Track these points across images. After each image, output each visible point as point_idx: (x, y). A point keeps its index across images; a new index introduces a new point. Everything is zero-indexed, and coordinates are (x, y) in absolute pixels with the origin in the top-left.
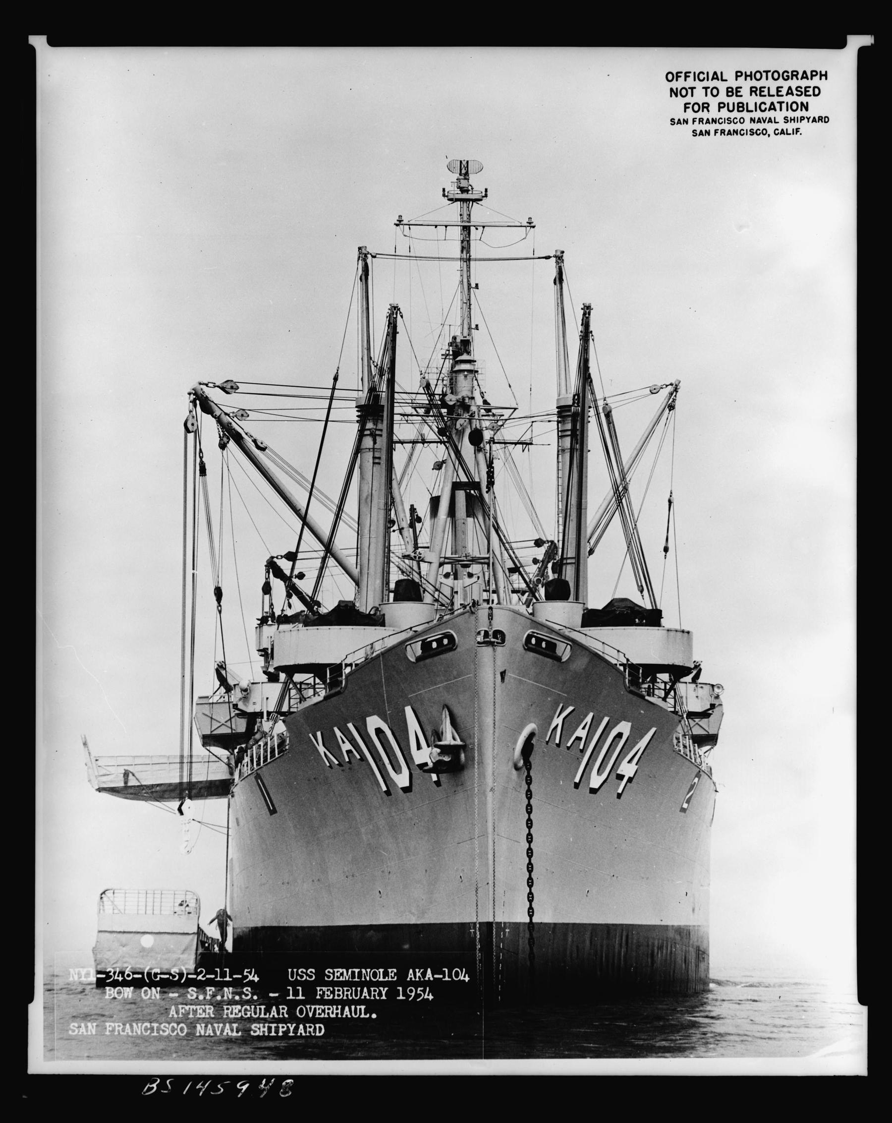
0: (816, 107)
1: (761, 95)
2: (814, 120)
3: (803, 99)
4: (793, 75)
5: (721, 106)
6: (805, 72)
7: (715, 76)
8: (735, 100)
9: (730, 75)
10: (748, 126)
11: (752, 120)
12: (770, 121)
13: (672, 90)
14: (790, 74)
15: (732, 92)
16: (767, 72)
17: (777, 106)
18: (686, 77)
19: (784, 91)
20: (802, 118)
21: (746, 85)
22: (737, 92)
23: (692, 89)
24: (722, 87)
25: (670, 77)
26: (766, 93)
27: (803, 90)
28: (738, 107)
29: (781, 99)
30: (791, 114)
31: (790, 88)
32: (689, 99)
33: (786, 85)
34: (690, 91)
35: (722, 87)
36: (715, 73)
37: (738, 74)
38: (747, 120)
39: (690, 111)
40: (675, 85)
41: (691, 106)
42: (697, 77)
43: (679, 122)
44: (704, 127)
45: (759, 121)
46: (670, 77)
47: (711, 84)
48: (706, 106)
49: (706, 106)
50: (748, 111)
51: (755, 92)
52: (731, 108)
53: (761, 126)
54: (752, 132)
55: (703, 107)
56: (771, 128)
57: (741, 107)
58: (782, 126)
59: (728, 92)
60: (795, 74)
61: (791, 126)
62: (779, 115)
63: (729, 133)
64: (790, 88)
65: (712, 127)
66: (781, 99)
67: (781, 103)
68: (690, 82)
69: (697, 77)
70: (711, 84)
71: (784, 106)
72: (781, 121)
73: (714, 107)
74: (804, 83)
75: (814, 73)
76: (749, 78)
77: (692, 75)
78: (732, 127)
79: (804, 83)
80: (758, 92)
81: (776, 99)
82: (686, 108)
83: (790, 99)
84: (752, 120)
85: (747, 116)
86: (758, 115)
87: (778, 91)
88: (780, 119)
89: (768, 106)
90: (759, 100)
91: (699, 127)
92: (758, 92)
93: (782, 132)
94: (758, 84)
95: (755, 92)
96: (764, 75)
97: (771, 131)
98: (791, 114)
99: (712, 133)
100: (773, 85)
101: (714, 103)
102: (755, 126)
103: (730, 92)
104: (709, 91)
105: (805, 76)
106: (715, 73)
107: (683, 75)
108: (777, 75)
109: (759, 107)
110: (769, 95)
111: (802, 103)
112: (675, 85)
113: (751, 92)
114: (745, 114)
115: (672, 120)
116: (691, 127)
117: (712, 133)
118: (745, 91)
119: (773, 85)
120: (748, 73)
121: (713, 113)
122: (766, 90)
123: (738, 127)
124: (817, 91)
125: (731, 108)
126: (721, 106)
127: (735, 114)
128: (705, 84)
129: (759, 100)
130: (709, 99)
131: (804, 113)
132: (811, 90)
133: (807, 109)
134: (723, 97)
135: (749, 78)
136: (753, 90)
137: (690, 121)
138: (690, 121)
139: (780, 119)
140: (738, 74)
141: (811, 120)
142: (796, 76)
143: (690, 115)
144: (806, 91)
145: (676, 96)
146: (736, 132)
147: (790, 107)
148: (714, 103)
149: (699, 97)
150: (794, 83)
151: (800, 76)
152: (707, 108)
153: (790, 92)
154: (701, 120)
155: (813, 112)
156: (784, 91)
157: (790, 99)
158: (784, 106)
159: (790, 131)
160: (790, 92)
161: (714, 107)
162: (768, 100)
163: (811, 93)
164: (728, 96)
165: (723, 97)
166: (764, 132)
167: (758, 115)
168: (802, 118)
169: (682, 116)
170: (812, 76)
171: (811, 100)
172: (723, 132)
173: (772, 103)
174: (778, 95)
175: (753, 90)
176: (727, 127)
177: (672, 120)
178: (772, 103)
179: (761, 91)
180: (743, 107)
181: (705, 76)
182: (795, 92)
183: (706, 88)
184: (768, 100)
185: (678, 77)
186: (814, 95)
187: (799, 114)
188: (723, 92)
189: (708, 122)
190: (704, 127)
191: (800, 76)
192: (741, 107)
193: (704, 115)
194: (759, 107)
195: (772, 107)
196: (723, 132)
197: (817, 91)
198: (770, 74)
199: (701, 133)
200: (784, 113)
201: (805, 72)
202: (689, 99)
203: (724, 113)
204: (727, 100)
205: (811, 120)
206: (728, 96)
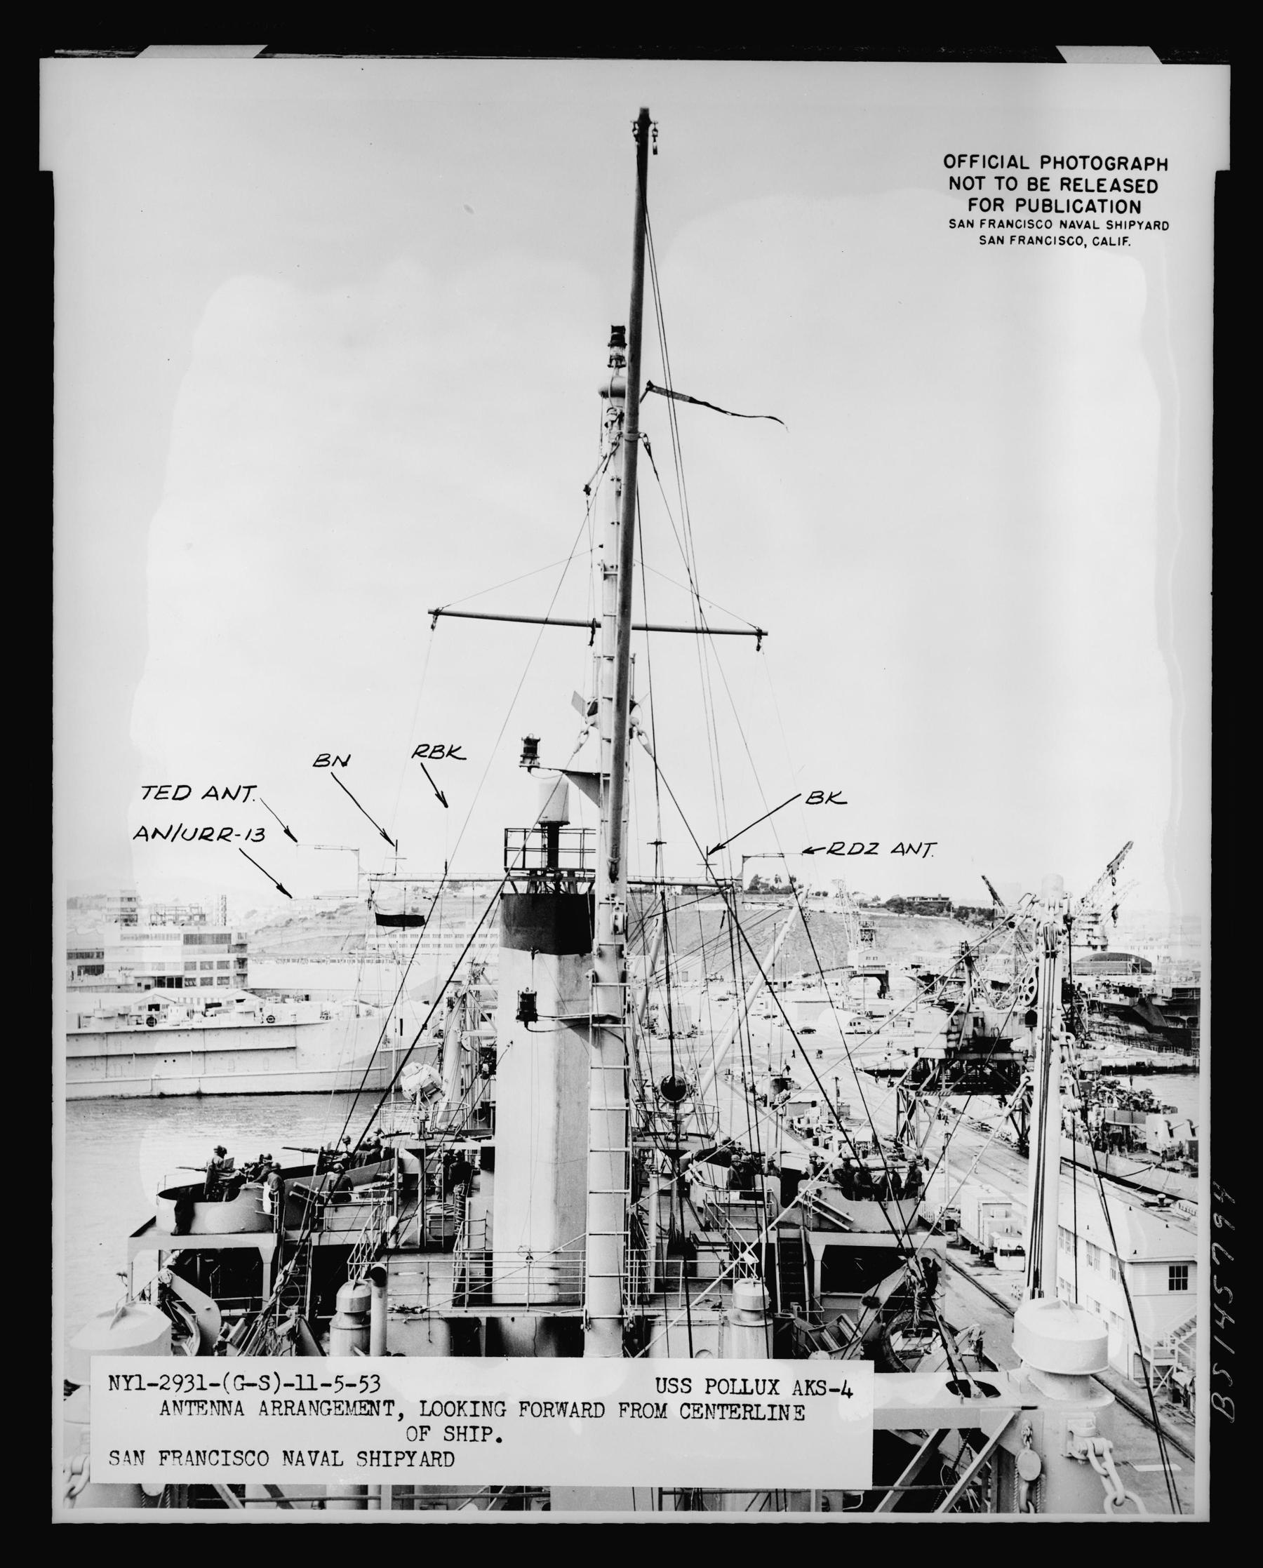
0: (1152, 207)
1: (1075, 190)
2: (1148, 226)
3: (1133, 196)
4: (1120, 163)
5: (1020, 203)
6: (1137, 159)
7: (1013, 162)
8: (1039, 195)
9: (1033, 162)
10: (1056, 231)
11: (1063, 224)
12: (1087, 225)
13: (952, 179)
14: (1116, 162)
15: (1035, 184)
16: (1084, 158)
17: (1098, 205)
18: (972, 161)
19: (1107, 185)
20: (1132, 224)
21: (1055, 175)
22: (1042, 184)
23: (980, 178)
24: (1022, 176)
25: (950, 161)
26: (1082, 187)
27: (1134, 184)
28: (1044, 205)
29: (1102, 196)
30: (1116, 218)
31: (1116, 181)
32: (975, 192)
33: (1110, 176)
34: (977, 181)
35: (1022, 176)
36: (1013, 158)
37: (1045, 160)
38: (1056, 224)
39: (976, 209)
40: (958, 172)
41: (978, 202)
42: (988, 162)
43: (961, 224)
44: (996, 232)
45: (1072, 225)
46: (950, 161)
47: (1007, 172)
48: (999, 204)
49: (999, 204)
50: (1057, 211)
51: (1068, 185)
52: (1033, 207)
53: (1075, 232)
54: (1063, 241)
55: (995, 205)
56: (1088, 235)
57: (1047, 205)
58: (1103, 232)
59: (1030, 184)
60: (1123, 162)
61: (1116, 234)
62: (1100, 218)
63: (1031, 241)
64: (1116, 181)
65: (1007, 232)
66: (1102, 196)
67: (1103, 201)
68: (978, 169)
69: (988, 162)
70: (1007, 172)
71: (1107, 205)
72: (1103, 226)
73: (1010, 205)
74: (1135, 175)
75: (1149, 162)
76: (1059, 166)
77: (980, 159)
78: (1035, 233)
79: (1135, 175)
80: (1071, 186)
81: (1096, 196)
82: (971, 205)
83: (1115, 196)
84: (1063, 224)
85: (1055, 218)
86: (1070, 217)
87: (1099, 185)
88: (1101, 223)
89: (1085, 205)
90: (1073, 196)
91: (989, 232)
92: (1071, 186)
93: (1104, 242)
94: (1072, 175)
95: (1068, 185)
96: (1081, 161)
97: (1088, 240)
98: (1116, 218)
99: (1007, 240)
100: (1092, 176)
101: (1010, 198)
102: (1067, 232)
103: (1033, 184)
104: (1004, 182)
105: (1136, 165)
106: (1013, 158)
107: (968, 159)
108: (1098, 162)
109: (1072, 206)
110: (1087, 190)
111: (1132, 203)
112: (958, 172)
113: (1062, 184)
114: (1053, 215)
115: (952, 221)
116: (977, 231)
117: (1007, 240)
118: (1053, 184)
119: (1092, 176)
120: (1059, 159)
121: (1009, 213)
122: (1083, 183)
123: (1043, 233)
124: (1153, 186)
125: (1033, 207)
126: (1020, 203)
127: (1039, 214)
128: (999, 172)
129: (1073, 196)
130: (1004, 193)
131: (1134, 216)
132: (1145, 184)
133: (1138, 211)
134: (1022, 191)
135: (1059, 166)
136: (1065, 183)
137: (977, 224)
138: (977, 224)
139: (1101, 223)
140: (1045, 160)
141: (1144, 226)
142: (1125, 164)
143: (976, 215)
144: (1138, 186)
145: (958, 187)
146: (1040, 240)
147: (1115, 207)
148: (1010, 198)
149: (990, 190)
150: (1121, 174)
151: (1129, 165)
152: (1000, 205)
153: (1115, 186)
154: (992, 222)
155: (1144, 216)
156: (1107, 185)
157: (1115, 196)
158: (1107, 205)
159: (1115, 241)
160: (1115, 186)
161: (1010, 205)
162: (1086, 197)
163: (1145, 188)
164: (1030, 189)
165: (1022, 191)
166: (1079, 241)
167: (1070, 217)
168: (1132, 224)
169: (966, 216)
170: (1147, 164)
171: (1145, 199)
172: (1022, 239)
173: (1091, 202)
174: (1099, 191)
175: (1065, 183)
176: (1027, 233)
177: (952, 221)
178: (1091, 202)
179: (1076, 184)
180: (1050, 205)
181: (999, 161)
182: (1122, 187)
183: (1000, 178)
184: (1086, 197)
185: (960, 161)
186: (1149, 191)
187: (1127, 217)
188: (1023, 184)
189: (1001, 225)
190: (996, 232)
191: (1129, 165)
192: (1047, 205)
193: (996, 215)
194: (1072, 206)
195: (1091, 207)
196: (1022, 239)
197: (1153, 186)
198: (1088, 161)
199: (992, 240)
200: (1108, 215)
201: (1137, 159)
202: (975, 192)
203: (1024, 214)
204: (1027, 195)
205: (1144, 226)
206: (1030, 189)
